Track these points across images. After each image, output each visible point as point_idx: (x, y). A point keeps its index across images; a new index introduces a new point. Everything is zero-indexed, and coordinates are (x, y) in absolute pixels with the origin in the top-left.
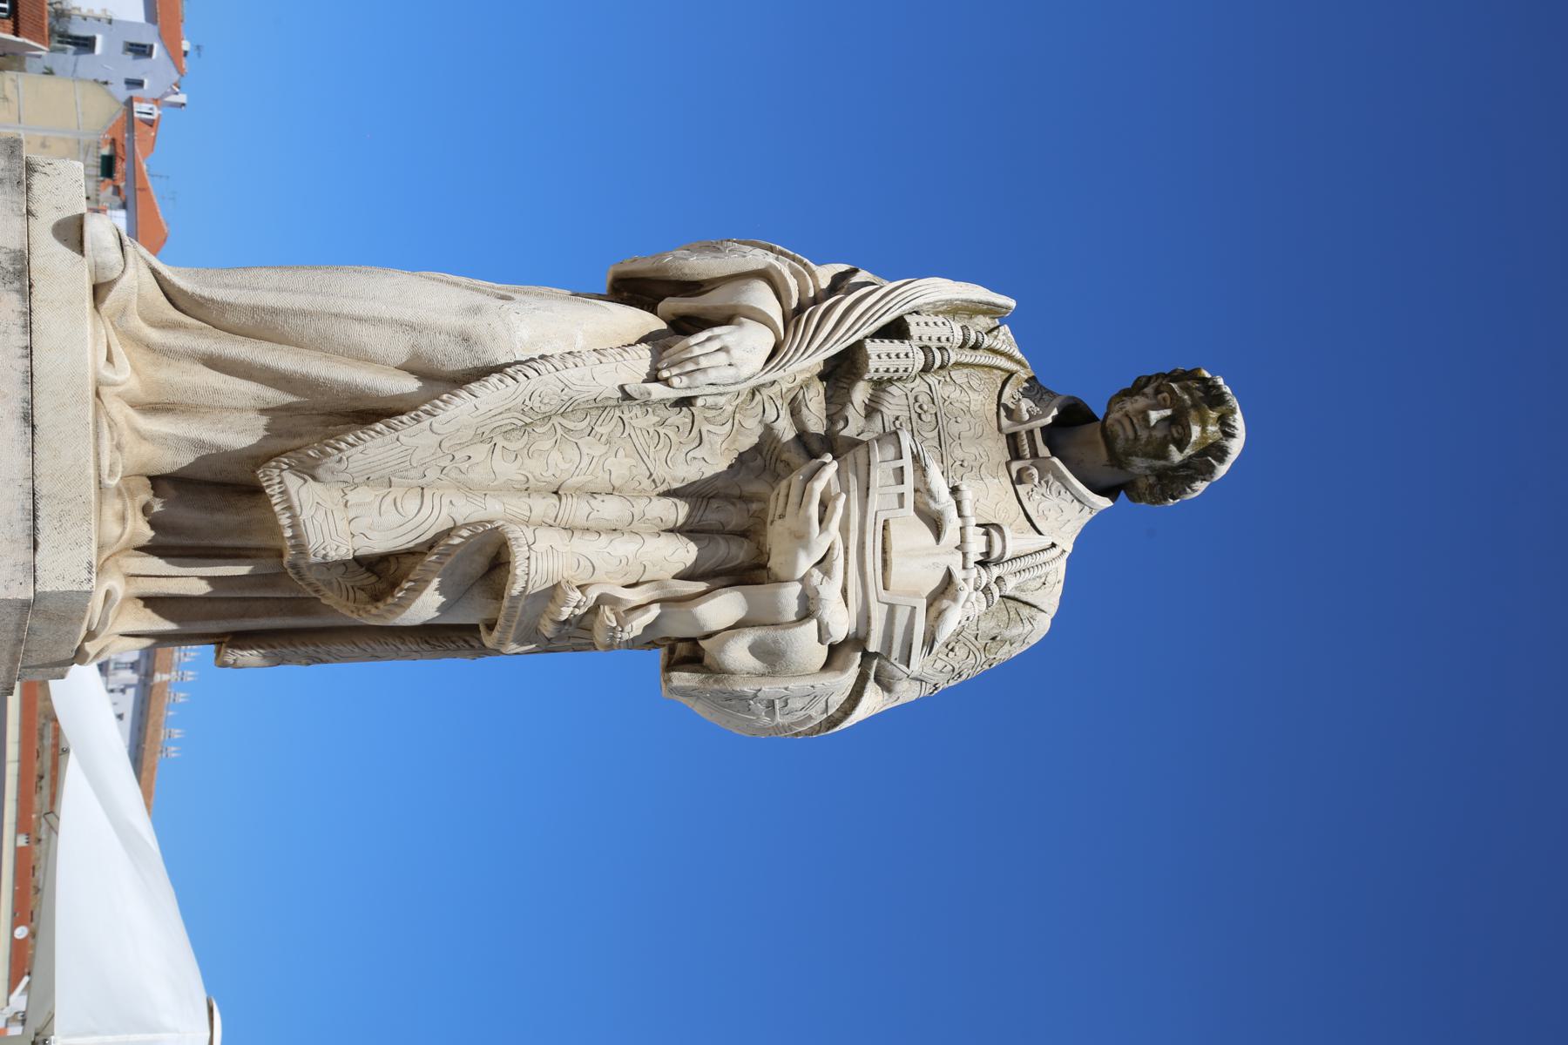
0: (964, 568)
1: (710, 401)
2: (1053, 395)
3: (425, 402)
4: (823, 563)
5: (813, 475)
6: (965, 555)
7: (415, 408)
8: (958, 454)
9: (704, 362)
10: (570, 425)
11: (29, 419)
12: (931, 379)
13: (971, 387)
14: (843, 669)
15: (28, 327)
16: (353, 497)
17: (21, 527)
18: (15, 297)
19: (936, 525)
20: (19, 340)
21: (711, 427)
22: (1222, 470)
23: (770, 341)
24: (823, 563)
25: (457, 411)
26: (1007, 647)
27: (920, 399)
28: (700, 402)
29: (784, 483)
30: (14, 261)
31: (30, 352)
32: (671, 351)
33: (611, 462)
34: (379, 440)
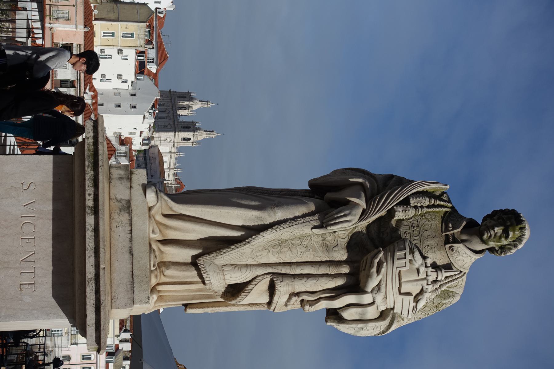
0: (427, 284)
1: (340, 232)
2: (462, 218)
3: (247, 239)
5: (375, 256)
6: (427, 280)
7: (244, 240)
8: (427, 243)
10: (294, 242)
11: (131, 253)
13: (432, 219)
14: (384, 319)
15: (131, 224)
17: (129, 287)
18: (127, 215)
20: (128, 228)
21: (341, 239)
22: (520, 247)
24: (379, 285)
25: (257, 241)
26: (444, 305)
27: (414, 225)
29: (365, 258)
30: (127, 203)
31: (131, 232)
32: (328, 216)
34: (233, 251)
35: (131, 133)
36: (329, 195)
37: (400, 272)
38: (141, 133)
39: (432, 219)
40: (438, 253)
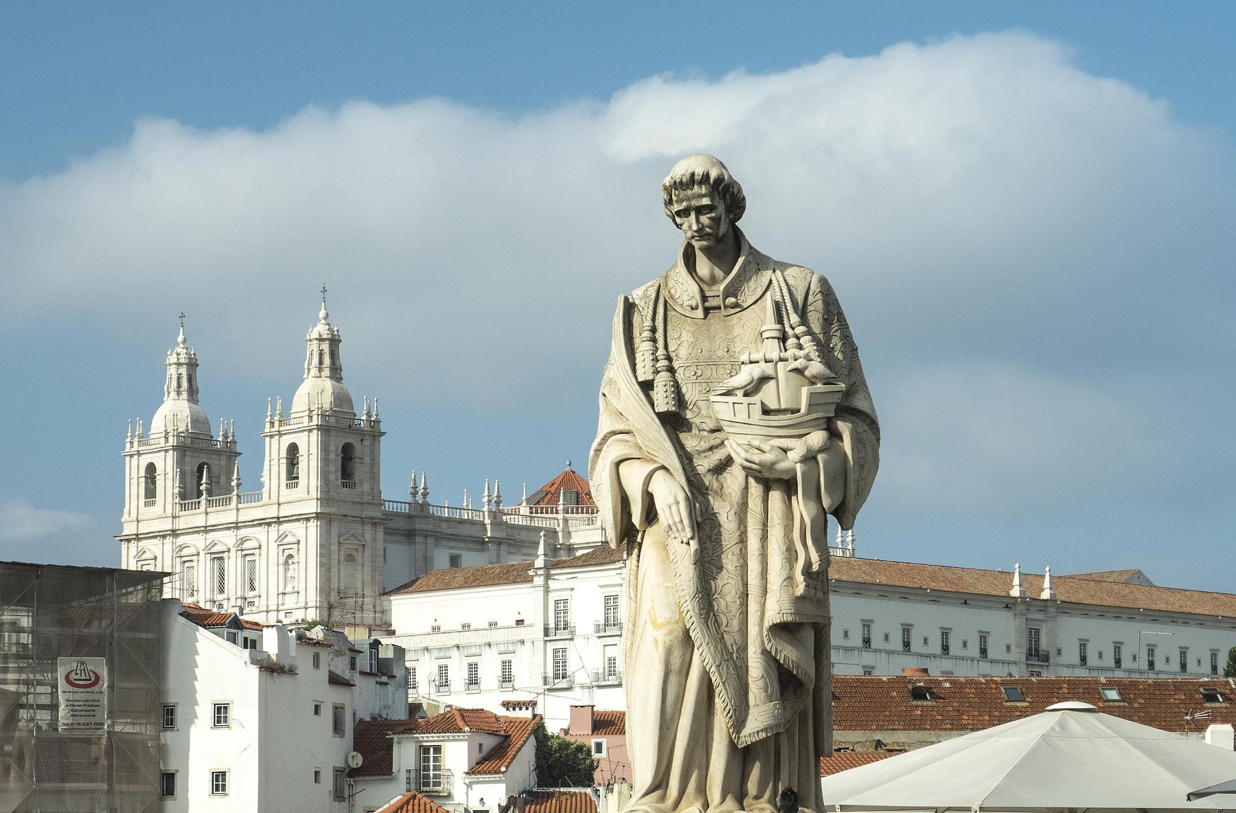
4: (785, 451)
9: (677, 519)
12: (676, 365)
16: (752, 702)
19: (764, 379)
23: (660, 476)
28: (699, 520)
33: (729, 567)
35: (338, 728)
36: (636, 519)
37: (766, 411)
38: (335, 680)
39: (679, 338)
40: (737, 331)
